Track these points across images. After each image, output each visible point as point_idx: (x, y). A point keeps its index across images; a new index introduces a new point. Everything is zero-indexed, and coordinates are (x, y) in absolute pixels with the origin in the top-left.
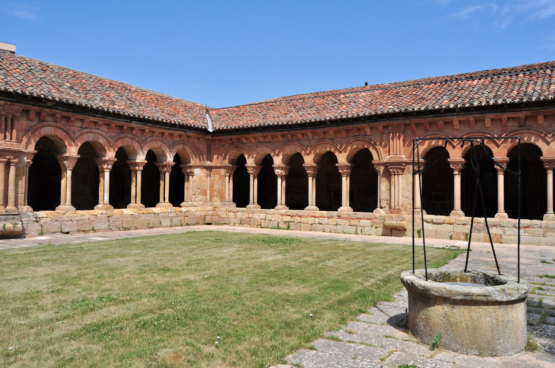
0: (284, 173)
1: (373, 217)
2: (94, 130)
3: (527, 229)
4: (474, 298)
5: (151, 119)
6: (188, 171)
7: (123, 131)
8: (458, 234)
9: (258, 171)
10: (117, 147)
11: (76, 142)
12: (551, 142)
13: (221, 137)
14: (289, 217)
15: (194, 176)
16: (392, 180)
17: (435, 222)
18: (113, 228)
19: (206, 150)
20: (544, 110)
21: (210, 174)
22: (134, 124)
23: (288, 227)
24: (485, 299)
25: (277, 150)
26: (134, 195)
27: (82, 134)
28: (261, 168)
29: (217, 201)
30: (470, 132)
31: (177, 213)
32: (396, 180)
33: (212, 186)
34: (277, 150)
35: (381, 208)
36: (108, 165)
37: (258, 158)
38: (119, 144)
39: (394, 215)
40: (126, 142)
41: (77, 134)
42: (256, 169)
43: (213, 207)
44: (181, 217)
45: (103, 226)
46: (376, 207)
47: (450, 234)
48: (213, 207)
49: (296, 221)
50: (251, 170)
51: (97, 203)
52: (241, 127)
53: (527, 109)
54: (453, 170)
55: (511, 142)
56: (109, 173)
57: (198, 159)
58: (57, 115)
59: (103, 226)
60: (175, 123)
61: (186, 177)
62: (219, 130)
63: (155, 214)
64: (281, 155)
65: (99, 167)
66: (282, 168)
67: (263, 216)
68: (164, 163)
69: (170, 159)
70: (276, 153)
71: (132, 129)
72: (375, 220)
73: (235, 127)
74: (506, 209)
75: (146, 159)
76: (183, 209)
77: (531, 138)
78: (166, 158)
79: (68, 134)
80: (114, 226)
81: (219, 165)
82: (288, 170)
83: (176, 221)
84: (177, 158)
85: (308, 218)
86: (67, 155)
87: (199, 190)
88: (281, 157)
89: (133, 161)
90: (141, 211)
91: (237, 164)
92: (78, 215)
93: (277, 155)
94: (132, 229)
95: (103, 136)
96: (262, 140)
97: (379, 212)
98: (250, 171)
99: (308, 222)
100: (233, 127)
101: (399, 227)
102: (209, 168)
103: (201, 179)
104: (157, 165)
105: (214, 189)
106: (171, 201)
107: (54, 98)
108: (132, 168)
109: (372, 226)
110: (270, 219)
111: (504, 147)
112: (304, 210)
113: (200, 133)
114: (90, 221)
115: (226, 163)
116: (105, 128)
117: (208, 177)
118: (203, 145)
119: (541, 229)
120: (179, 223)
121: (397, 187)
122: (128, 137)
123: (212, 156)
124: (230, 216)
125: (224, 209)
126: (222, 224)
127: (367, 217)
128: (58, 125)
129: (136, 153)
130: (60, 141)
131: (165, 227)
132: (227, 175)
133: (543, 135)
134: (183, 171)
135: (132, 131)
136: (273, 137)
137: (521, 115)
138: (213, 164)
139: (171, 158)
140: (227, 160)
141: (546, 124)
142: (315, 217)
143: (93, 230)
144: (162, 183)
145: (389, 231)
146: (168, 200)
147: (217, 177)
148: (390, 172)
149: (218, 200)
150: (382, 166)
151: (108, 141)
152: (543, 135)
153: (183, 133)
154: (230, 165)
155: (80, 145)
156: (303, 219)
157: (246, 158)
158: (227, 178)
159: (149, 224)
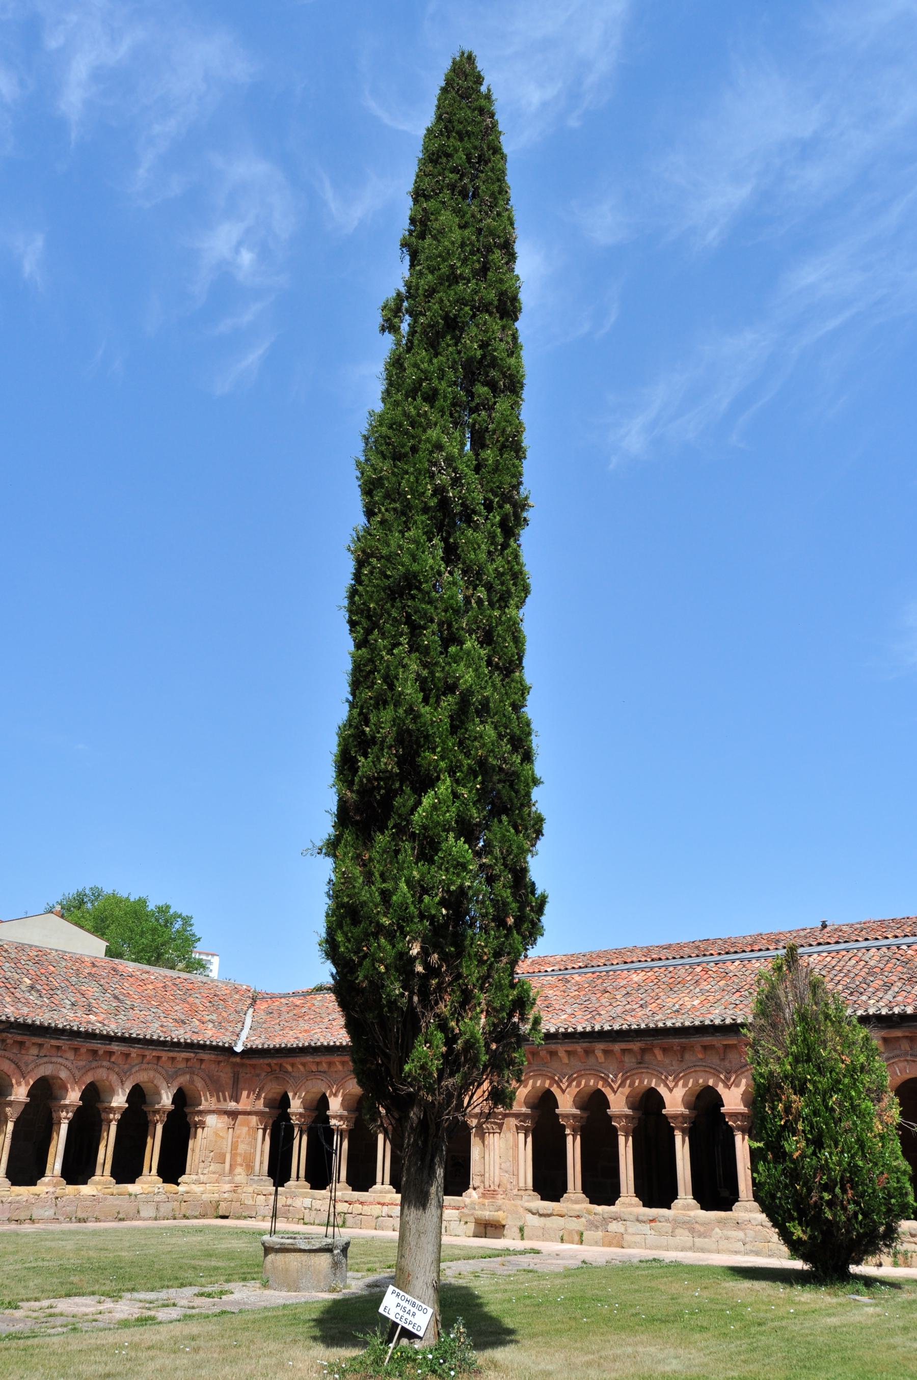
0: (344, 1126)
1: (462, 1205)
2: (54, 1059)
3: (653, 1224)
4: (286, 1246)
5: (141, 1037)
6: (197, 1119)
7: (97, 1058)
8: (570, 1232)
9: (309, 1120)
10: (84, 1083)
11: (27, 1078)
12: (673, 1088)
13: (254, 1061)
14: (346, 1204)
15: (206, 1129)
16: (486, 1143)
17: (541, 1213)
18: (62, 1218)
19: (231, 1082)
20: (659, 1041)
21: (234, 1125)
22: (115, 1047)
23: (344, 1222)
24: (291, 1247)
25: (335, 1086)
26: (102, 1161)
27: (38, 1066)
28: (314, 1115)
29: (240, 1175)
30: (582, 1068)
31: (168, 1194)
32: (491, 1142)
33: (234, 1147)
34: (335, 1086)
35: (475, 1189)
36: (67, 1113)
37: (308, 1097)
38: (88, 1079)
39: (486, 1201)
40: (101, 1074)
41: (31, 1067)
42: (304, 1118)
43: (233, 1185)
44: (176, 1203)
45: (47, 1213)
46: (468, 1188)
47: (561, 1233)
48: (233, 1185)
49: (355, 1212)
50: (296, 1119)
51: (42, 1174)
52: (283, 1046)
53: (639, 1039)
54: (564, 1127)
55: (630, 1086)
56: (67, 1125)
57: (214, 1099)
58: (9, 1041)
59: (47, 1213)
60: (179, 1040)
61: (193, 1130)
62: (251, 1048)
63: (130, 1195)
64: (340, 1094)
65: (54, 1115)
66: (341, 1118)
67: (307, 1202)
68: (157, 1106)
69: (166, 1100)
70: (334, 1091)
71: (111, 1053)
72: (465, 1211)
73: (275, 1046)
74: (639, 1193)
75: (127, 1102)
76: (181, 1188)
77: (652, 1081)
78: (161, 1098)
79: (18, 1067)
80: (63, 1214)
81: (248, 1108)
82: (353, 1120)
83: (165, 1209)
84: (180, 1098)
85: (373, 1206)
86: (12, 1098)
87: (212, 1153)
88: (340, 1099)
89: (106, 1105)
90: (109, 1190)
91: (279, 1108)
92: (13, 1195)
93: (335, 1095)
94: (91, 1221)
95: (66, 1067)
96: (314, 1068)
97: (471, 1196)
98: (294, 1120)
99: (373, 1214)
100: (272, 1046)
101: (493, 1221)
102: (233, 1115)
103: (216, 1134)
104: (145, 1109)
105: (239, 1151)
106: (160, 1173)
107: (8, 1018)
108: (104, 1115)
109: (460, 1221)
110: (318, 1208)
111: (622, 1093)
112: (367, 1191)
113: (221, 1055)
114: (29, 1205)
115: (260, 1105)
116: (70, 1055)
117: (231, 1130)
118: (226, 1073)
119: (669, 1224)
120: (171, 1215)
121: (492, 1154)
122: (103, 1067)
123: (239, 1093)
124: (258, 1203)
125: (250, 1189)
126: (245, 1217)
127: (454, 1205)
128: (7, 1054)
129: (112, 1092)
130: (7, 1077)
131: (145, 1220)
132: (260, 1127)
133: (663, 1077)
134: (188, 1119)
135: (110, 1057)
136: (330, 1064)
137: (636, 1046)
138: (240, 1107)
139: (168, 1098)
140: (262, 1100)
141: (667, 1061)
142: (383, 1204)
143: (30, 1219)
144: (149, 1140)
145: (482, 1229)
146: (156, 1171)
147: (245, 1130)
148: (483, 1129)
149: (244, 1173)
150: (475, 1118)
151: (73, 1075)
152: (663, 1077)
153: (192, 1055)
154: (267, 1110)
155: (32, 1082)
156: (365, 1207)
157: (291, 1098)
158: (261, 1132)
159: (118, 1213)
